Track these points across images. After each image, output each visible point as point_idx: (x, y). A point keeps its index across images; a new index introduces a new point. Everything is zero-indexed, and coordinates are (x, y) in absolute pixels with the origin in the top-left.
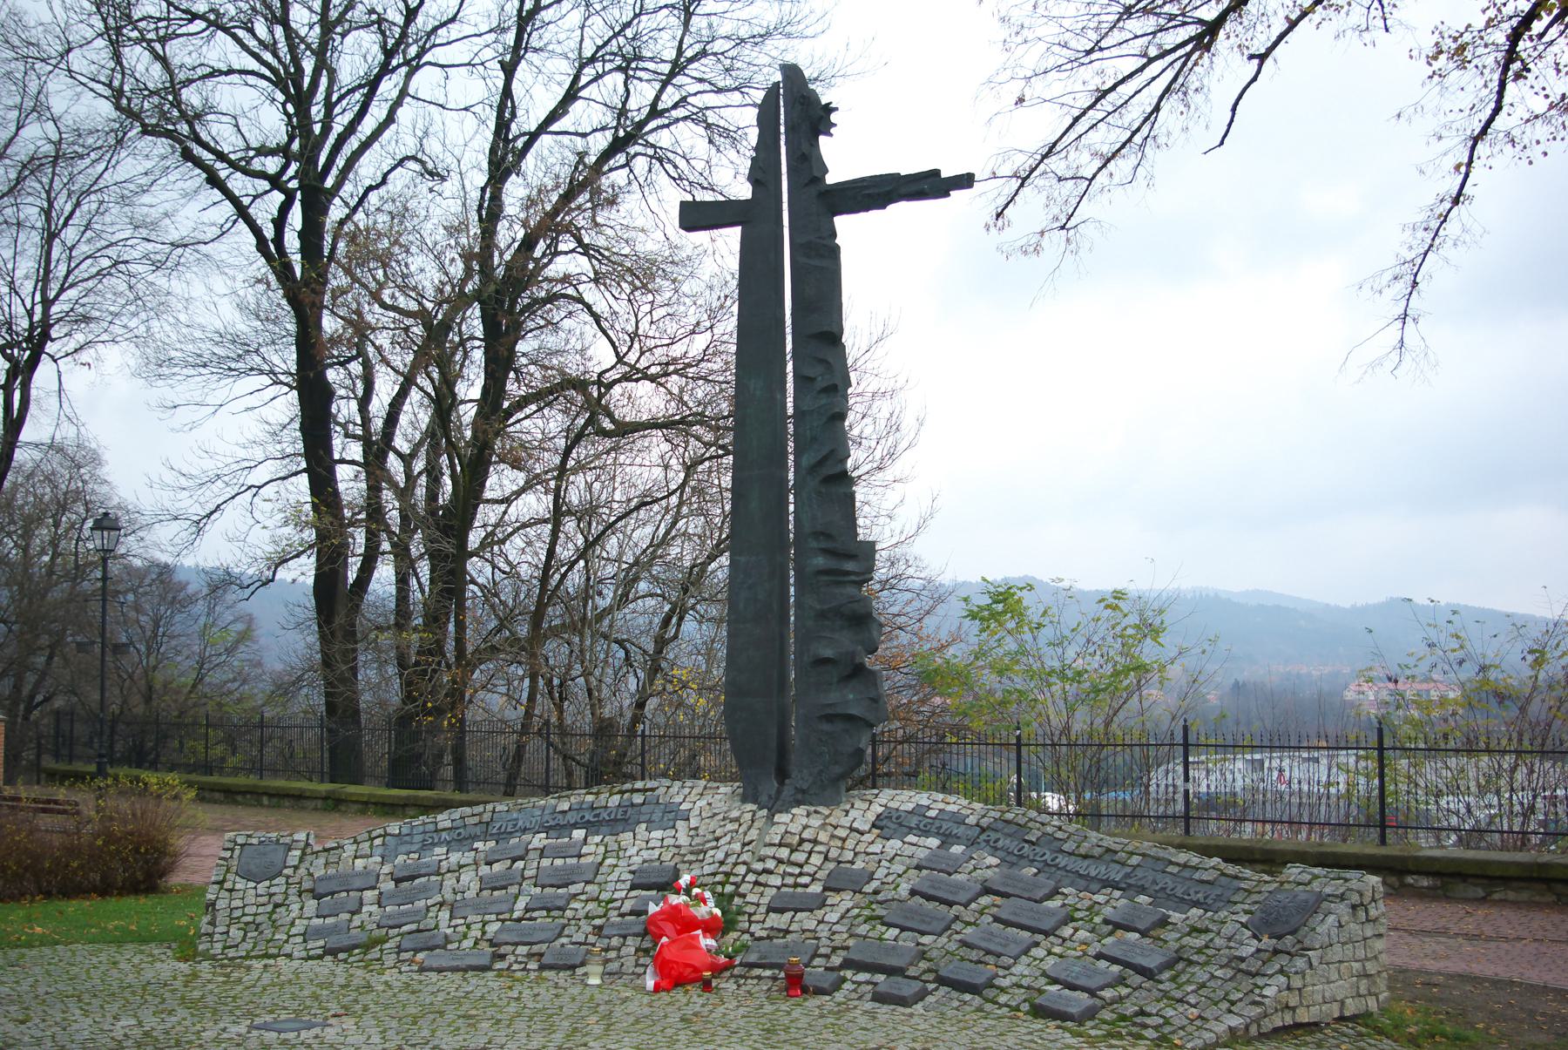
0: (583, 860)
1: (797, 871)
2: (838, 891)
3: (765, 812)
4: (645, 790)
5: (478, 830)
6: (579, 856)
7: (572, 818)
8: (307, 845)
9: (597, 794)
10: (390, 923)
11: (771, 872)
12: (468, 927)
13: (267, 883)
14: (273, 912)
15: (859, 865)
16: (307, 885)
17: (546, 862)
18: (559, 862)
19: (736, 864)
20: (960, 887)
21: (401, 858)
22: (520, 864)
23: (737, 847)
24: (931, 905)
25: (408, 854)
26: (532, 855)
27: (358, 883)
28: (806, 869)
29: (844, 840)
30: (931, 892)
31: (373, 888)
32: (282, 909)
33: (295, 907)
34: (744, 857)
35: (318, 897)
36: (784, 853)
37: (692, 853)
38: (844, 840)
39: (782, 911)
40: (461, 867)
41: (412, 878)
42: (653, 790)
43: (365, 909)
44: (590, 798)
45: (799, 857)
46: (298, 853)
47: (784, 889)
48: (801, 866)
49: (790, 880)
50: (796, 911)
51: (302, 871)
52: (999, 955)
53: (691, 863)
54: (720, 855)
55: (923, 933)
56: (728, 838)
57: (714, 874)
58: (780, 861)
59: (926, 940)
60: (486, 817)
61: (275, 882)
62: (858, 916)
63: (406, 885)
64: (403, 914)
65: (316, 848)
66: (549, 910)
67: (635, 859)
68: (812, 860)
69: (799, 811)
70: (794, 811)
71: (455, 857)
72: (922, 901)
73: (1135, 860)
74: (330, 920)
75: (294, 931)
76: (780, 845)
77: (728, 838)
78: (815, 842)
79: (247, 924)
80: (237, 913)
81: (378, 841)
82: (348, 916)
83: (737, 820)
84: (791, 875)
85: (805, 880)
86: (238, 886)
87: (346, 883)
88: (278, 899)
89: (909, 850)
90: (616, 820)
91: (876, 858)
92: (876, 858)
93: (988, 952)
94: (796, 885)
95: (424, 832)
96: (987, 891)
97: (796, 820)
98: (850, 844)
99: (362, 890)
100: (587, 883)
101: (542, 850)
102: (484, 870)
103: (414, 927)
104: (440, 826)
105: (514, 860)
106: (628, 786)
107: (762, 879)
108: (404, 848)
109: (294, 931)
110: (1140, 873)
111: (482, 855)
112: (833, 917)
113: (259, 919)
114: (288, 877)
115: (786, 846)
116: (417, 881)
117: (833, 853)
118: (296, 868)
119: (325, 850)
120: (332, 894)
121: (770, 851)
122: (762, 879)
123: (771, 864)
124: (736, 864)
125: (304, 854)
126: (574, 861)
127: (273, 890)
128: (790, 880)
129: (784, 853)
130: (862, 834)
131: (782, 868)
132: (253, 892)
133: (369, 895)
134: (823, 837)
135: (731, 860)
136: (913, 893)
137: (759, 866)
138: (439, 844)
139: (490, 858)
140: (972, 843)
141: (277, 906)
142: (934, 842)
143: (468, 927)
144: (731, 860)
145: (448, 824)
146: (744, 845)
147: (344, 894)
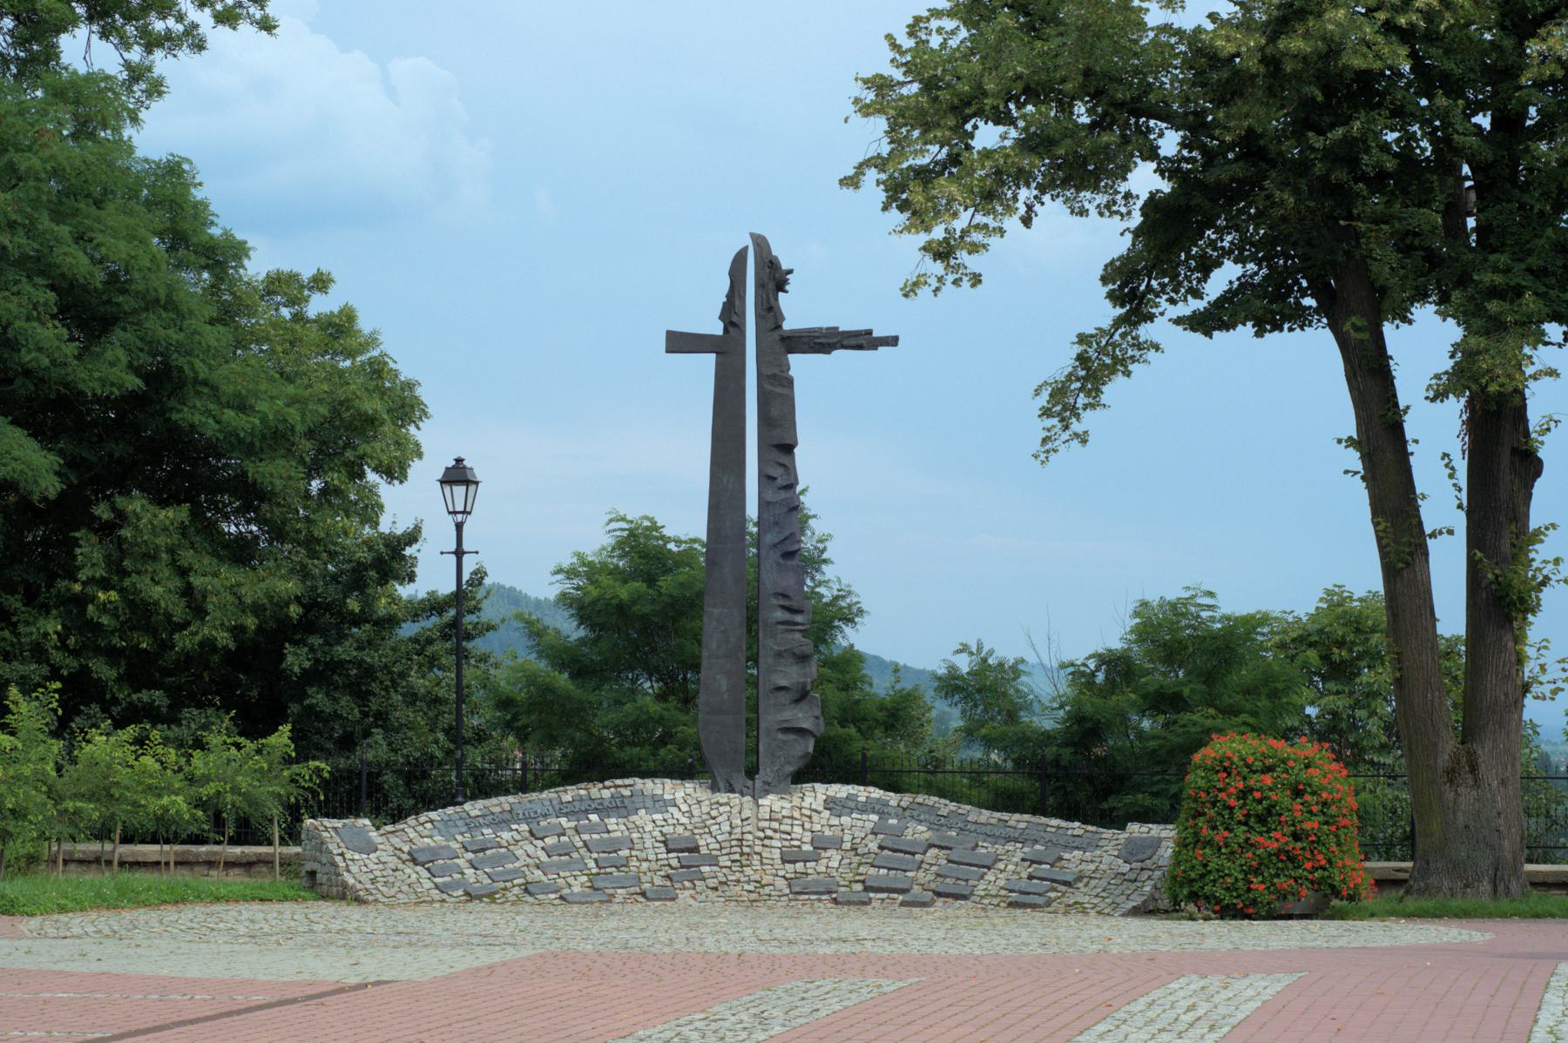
5: (508, 816)
15: (828, 833)
17: (586, 837)
18: (595, 836)
20: (914, 843)
26: (569, 832)
36: (775, 825)
39: (794, 862)
45: (788, 828)
58: (775, 831)
69: (771, 797)
73: (1022, 825)
77: (725, 817)
78: (792, 818)
83: (727, 804)
85: (796, 843)
89: (860, 823)
112: (836, 864)
117: (807, 826)
121: (766, 824)
122: (767, 842)
123: (769, 833)
129: (775, 825)
134: (796, 814)
135: (738, 830)
136: (881, 848)
137: (761, 834)
142: (875, 818)
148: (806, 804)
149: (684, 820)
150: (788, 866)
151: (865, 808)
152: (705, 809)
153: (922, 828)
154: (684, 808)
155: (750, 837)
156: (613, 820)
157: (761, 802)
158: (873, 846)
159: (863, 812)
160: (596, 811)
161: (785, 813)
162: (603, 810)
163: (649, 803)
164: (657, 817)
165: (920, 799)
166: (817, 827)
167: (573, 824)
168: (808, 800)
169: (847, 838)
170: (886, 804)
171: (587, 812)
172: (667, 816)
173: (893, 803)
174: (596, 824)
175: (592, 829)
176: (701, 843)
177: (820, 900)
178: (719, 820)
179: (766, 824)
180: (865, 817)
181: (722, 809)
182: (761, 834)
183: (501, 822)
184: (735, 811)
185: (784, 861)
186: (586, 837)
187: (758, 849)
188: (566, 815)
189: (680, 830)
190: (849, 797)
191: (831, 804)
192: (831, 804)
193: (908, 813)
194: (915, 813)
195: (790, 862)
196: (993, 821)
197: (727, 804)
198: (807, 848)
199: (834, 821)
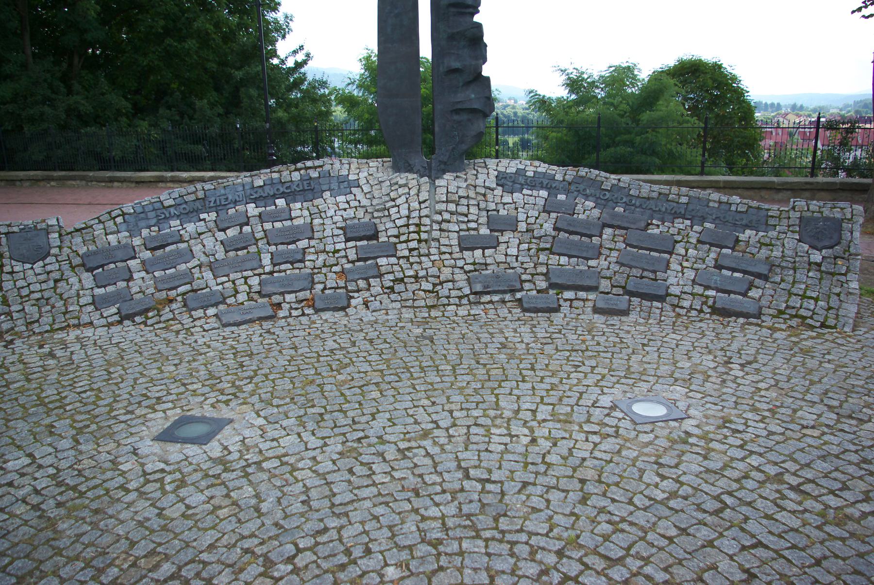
0: (296, 222)
1: (466, 219)
2: (502, 231)
3: (426, 179)
4: (315, 168)
5: (198, 205)
6: (292, 219)
7: (269, 190)
8: (60, 227)
9: (279, 172)
10: (166, 286)
11: (449, 222)
12: (233, 282)
13: (41, 263)
14: (55, 288)
15: (503, 212)
16: (77, 261)
17: (268, 226)
18: (278, 225)
19: (420, 217)
20: (587, 223)
21: (145, 232)
22: (247, 229)
23: (415, 205)
24: (576, 238)
25: (149, 227)
27: (120, 255)
28: (471, 217)
29: (484, 195)
30: (571, 229)
31: (134, 258)
32: (62, 284)
33: (73, 280)
34: (425, 212)
35: (90, 270)
36: (452, 207)
37: (377, 211)
38: (484, 195)
39: (472, 249)
40: (200, 234)
41: (163, 247)
42: (321, 167)
43: (135, 276)
44: (275, 175)
45: (463, 209)
46: (57, 235)
47: (462, 233)
48: (466, 216)
49: (464, 226)
50: (484, 249)
51: (66, 251)
52: (655, 272)
53: (380, 218)
54: (404, 212)
55: (587, 259)
56: (403, 199)
57: (407, 226)
58: (452, 213)
59: (592, 263)
60: (201, 194)
61: (47, 261)
62: (529, 250)
63: (159, 253)
64: (172, 277)
65: (69, 230)
66: (292, 263)
67: (336, 219)
68: (471, 211)
69: (448, 176)
70: (445, 176)
71: (191, 227)
72: (567, 235)
73: (684, 200)
74: (110, 289)
75: (83, 301)
76: (447, 202)
77: (403, 199)
78: (468, 197)
79: (38, 300)
80: (25, 292)
81: (119, 220)
82: (124, 284)
83: (406, 185)
84: (463, 222)
85: (473, 225)
86: (16, 269)
87: (108, 255)
88: (56, 275)
89: (531, 200)
90: (304, 190)
91: (513, 206)
92: (513, 206)
93: (644, 270)
94: (468, 229)
95: (154, 210)
96: (605, 225)
97: (448, 182)
98: (490, 197)
99: (126, 261)
100: (311, 238)
101: (260, 216)
102: (221, 236)
103: (187, 287)
104: (166, 204)
105: (241, 226)
106: (299, 165)
107: (444, 226)
108: (142, 224)
109: (83, 301)
110: (690, 207)
111: (212, 225)
112: (513, 251)
113: (46, 294)
114: (56, 256)
115: (452, 202)
116: (168, 249)
117: (483, 205)
118: (60, 247)
119: (77, 230)
120: (102, 266)
121: (443, 207)
122: (444, 226)
123: (446, 216)
124: (420, 217)
125: (60, 235)
126: (288, 223)
127: (49, 268)
128: (464, 226)
129: (452, 207)
130: (493, 190)
131: (455, 217)
132: (31, 272)
133: (132, 263)
134: (472, 194)
135: (415, 214)
137: (438, 218)
138: (171, 217)
139: (221, 226)
140: (567, 192)
141: (56, 281)
142: (544, 193)
143: (233, 282)
144: (415, 214)
145: (171, 202)
146: (420, 203)
147: (112, 266)
148: (480, 182)
149: (365, 202)
150: (467, 254)
151: (535, 183)
152: (385, 190)
153: (590, 204)
154: (366, 189)
155: (426, 221)
156: (298, 205)
157: (437, 182)
158: (548, 227)
159: (532, 187)
160: (283, 195)
161: (462, 193)
162: (291, 195)
163: (334, 185)
164: (341, 199)
165: (583, 171)
166: (492, 206)
167: (257, 212)
168: (482, 177)
169: (522, 217)
170: (553, 178)
171: (275, 197)
172: (350, 197)
173: (559, 177)
174: (283, 210)
175: (275, 217)
176: (381, 228)
177: (503, 302)
178: (398, 202)
179: (443, 207)
180: (535, 193)
181: (401, 191)
182: (438, 218)
183: (190, 213)
184: (413, 192)
185: (462, 249)
186: (268, 226)
187: (436, 234)
188: (254, 201)
189: (360, 213)
190: (520, 172)
191: (502, 179)
192: (502, 179)
193: (573, 188)
194: (581, 187)
195: (467, 249)
196: (655, 195)
197: (406, 185)
198: (484, 231)
199: (507, 199)
